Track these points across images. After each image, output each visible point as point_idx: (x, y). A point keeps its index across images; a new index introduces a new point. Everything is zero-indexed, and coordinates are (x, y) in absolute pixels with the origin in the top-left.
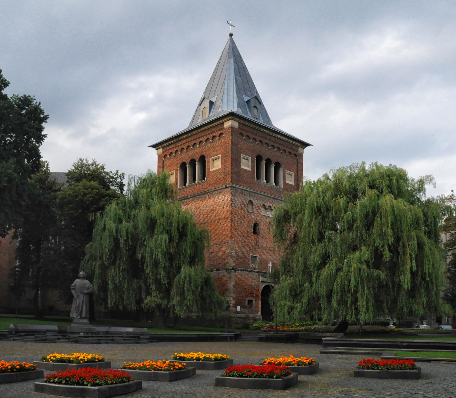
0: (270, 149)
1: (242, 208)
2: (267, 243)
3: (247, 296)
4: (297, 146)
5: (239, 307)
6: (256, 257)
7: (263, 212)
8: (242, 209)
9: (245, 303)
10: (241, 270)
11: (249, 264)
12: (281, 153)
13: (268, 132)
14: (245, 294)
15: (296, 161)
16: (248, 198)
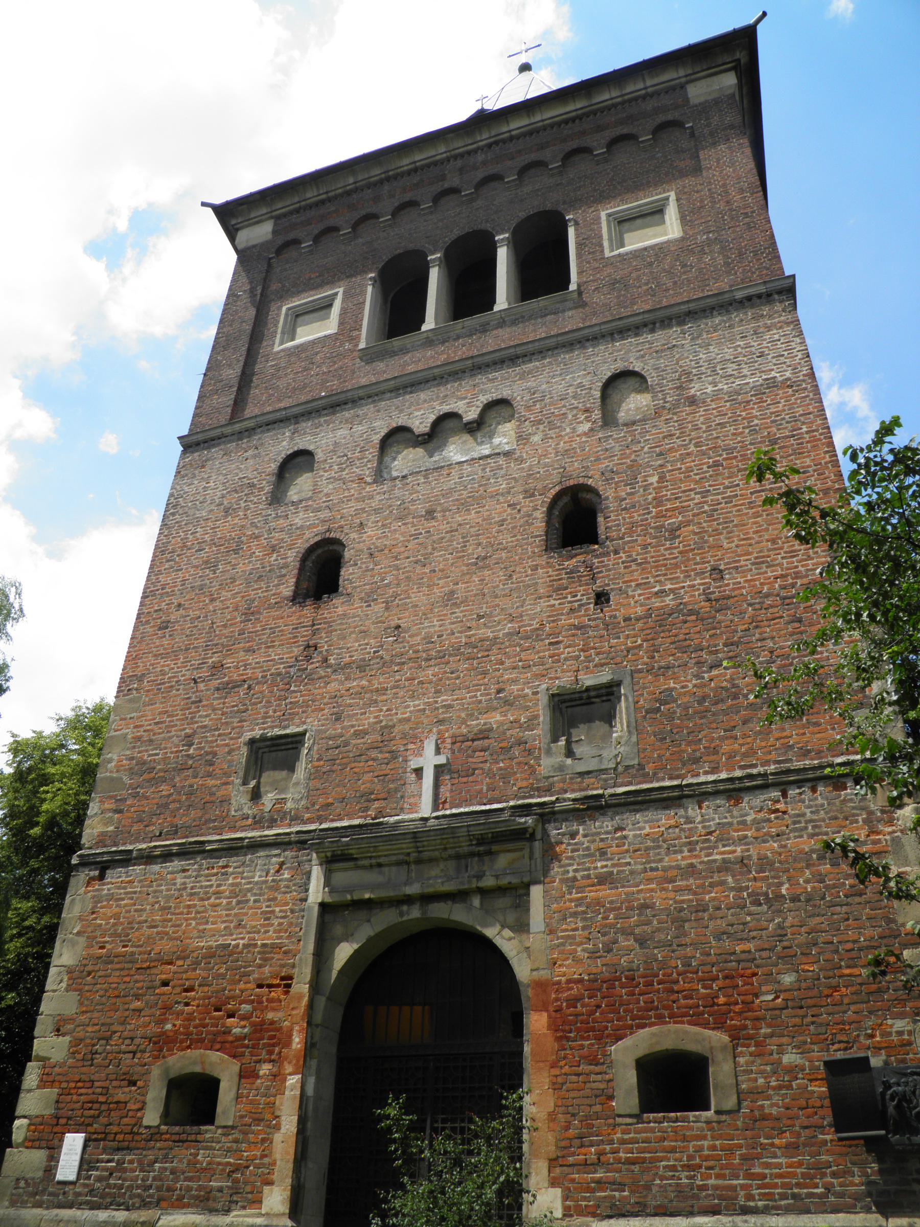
1: (226, 511)
5: (73, 1142)
6: (296, 741)
11: (226, 801)
14: (153, 1029)
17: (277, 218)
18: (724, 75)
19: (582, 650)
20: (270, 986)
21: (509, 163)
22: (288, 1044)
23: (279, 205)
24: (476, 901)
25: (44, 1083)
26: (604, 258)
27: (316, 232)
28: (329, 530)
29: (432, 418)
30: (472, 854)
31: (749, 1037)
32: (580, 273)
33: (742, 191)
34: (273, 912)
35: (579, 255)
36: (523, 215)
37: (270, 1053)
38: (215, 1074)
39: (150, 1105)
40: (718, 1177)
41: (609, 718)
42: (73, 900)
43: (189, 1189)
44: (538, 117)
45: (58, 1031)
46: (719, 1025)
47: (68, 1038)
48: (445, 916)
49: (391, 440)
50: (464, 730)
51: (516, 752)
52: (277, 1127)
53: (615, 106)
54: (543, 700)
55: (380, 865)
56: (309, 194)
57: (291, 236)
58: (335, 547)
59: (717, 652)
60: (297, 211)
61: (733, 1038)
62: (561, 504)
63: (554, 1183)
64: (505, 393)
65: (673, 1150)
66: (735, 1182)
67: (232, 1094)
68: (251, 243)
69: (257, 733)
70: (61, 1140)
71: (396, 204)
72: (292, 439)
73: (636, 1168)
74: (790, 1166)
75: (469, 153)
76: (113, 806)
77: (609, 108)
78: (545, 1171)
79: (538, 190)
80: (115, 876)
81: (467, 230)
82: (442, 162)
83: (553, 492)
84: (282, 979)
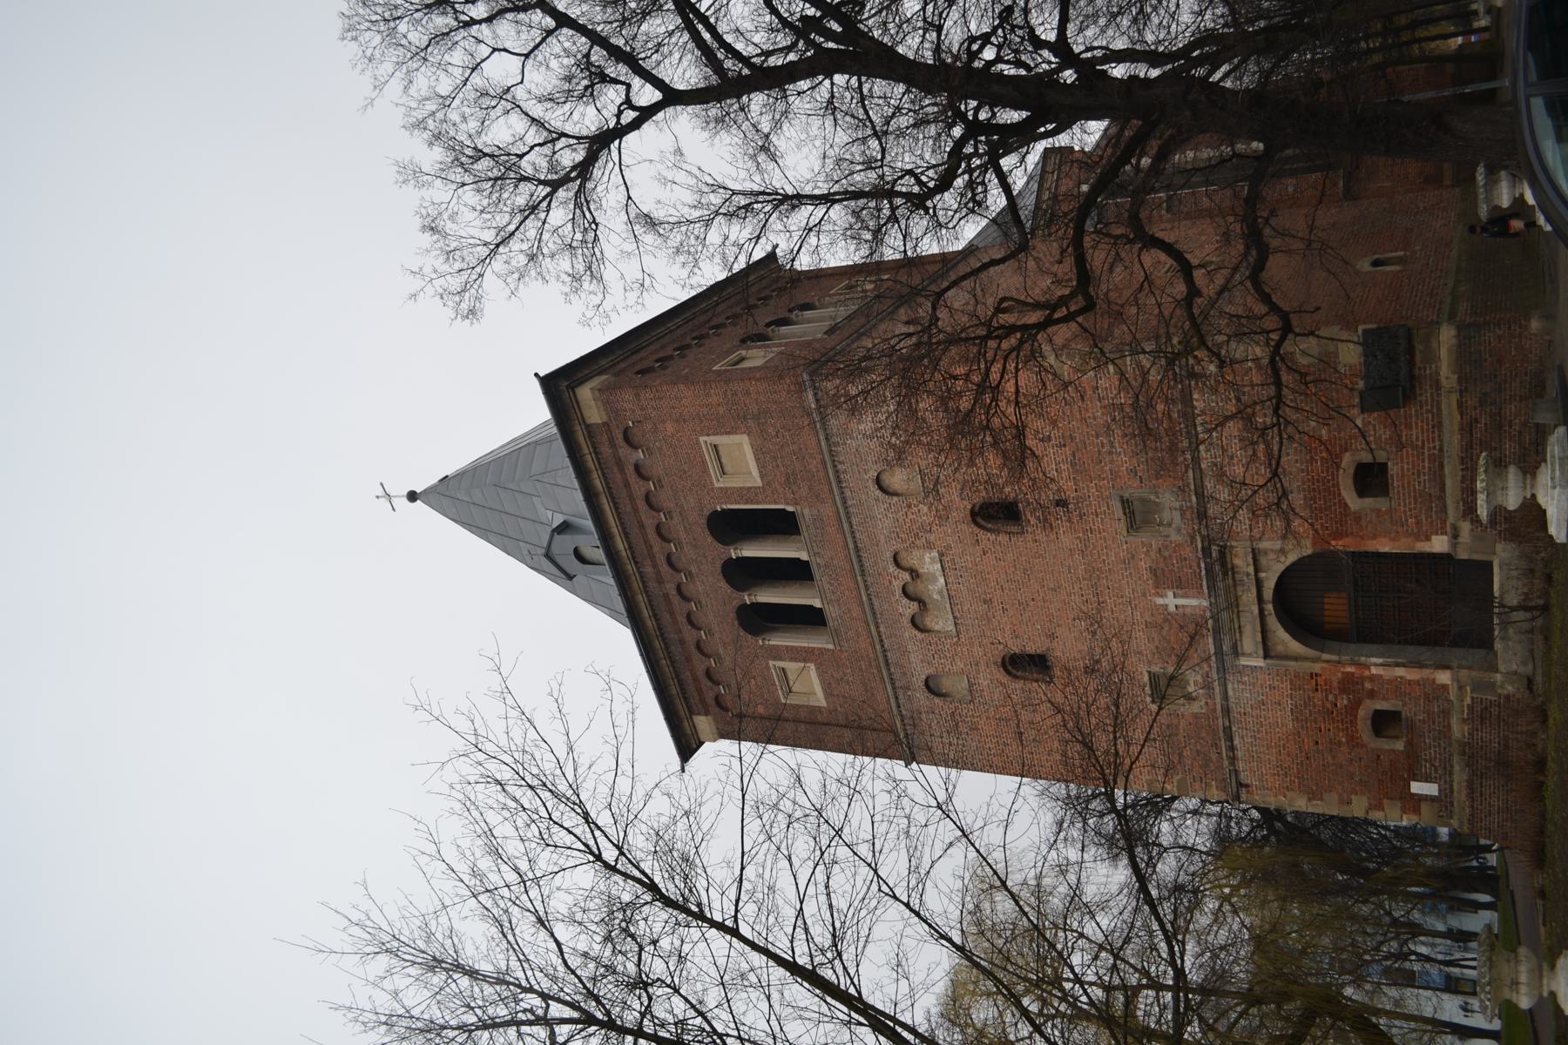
0: (690, 573)
2: (1072, 616)
3: (1354, 743)
4: (589, 429)
5: (1417, 788)
7: (941, 622)
8: (977, 729)
9: (1393, 751)
10: (1233, 760)
11: (1195, 716)
12: (669, 514)
13: (641, 599)
14: (1344, 749)
15: (648, 426)
16: (921, 697)
17: (691, 713)
18: (578, 397)
19: (1097, 516)
20: (1317, 685)
21: (656, 549)
22: (1353, 674)
23: (682, 713)
24: (1262, 575)
25: (1380, 807)
26: (763, 488)
27: (710, 684)
28: (995, 663)
29: (905, 601)
30: (1233, 578)
31: (1346, 444)
32: (776, 503)
33: (708, 395)
34: (1270, 685)
35: (757, 503)
36: (710, 539)
37: (1357, 683)
38: (1372, 712)
39: (1392, 747)
40: (1423, 461)
41: (1144, 501)
42: (1264, 802)
43: (1439, 722)
44: (615, 530)
45: (1349, 803)
46: (1339, 456)
47: (1353, 797)
48: (1271, 592)
49: (921, 626)
50: (1150, 582)
51: (1167, 554)
52: (1401, 677)
53: (604, 474)
54: (1130, 539)
55: (1240, 627)
56: (674, 692)
57: (711, 701)
58: (1007, 660)
59: (1102, 443)
60: (685, 698)
61: (1346, 450)
62: (982, 522)
63: (1428, 539)
64: (889, 555)
65: (1409, 482)
66: (1426, 454)
67: (1384, 703)
68: (715, 731)
69: (1149, 699)
70: (1415, 794)
71: (689, 627)
72: (914, 690)
73: (1419, 500)
74: (1417, 428)
75: (642, 577)
76: (1198, 783)
77: (605, 478)
78: (1423, 543)
79: (685, 528)
80: (1245, 777)
81: (721, 577)
82: (648, 596)
83: (975, 528)
84: (1312, 678)
